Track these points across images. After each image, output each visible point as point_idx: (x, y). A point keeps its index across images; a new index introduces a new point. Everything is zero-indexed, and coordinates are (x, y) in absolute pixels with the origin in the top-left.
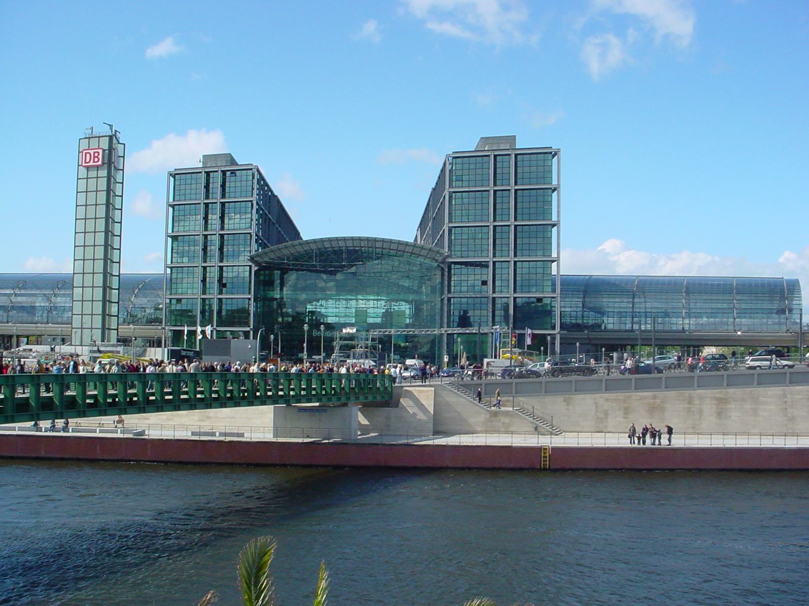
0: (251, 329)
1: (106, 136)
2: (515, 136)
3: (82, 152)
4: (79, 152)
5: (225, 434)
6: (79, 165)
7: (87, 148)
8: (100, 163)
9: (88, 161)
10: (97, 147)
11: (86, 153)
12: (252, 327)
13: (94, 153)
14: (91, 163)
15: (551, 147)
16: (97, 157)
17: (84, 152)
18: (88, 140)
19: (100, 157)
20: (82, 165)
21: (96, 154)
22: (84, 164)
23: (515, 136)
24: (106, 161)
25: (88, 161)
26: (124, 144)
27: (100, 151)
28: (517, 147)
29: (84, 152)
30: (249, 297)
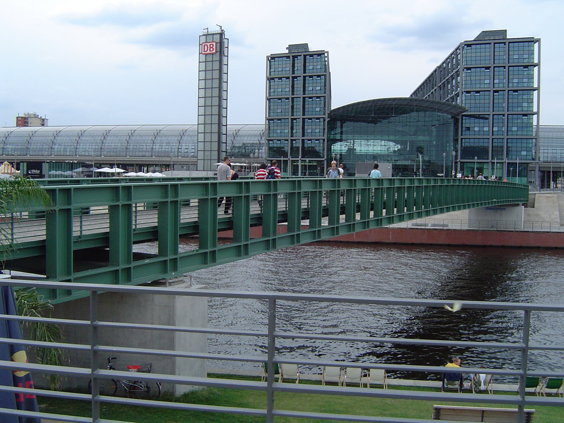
0: (325, 159)
1: (218, 34)
2: (506, 30)
3: (202, 44)
4: (200, 45)
5: (434, 225)
6: (200, 53)
7: (205, 42)
8: (214, 51)
9: (206, 50)
10: (212, 41)
11: (204, 45)
12: (326, 158)
13: (210, 45)
14: (208, 52)
15: (533, 38)
16: (212, 48)
17: (203, 44)
18: (205, 36)
19: (214, 47)
20: (202, 53)
21: (212, 46)
22: (203, 53)
23: (506, 30)
24: (218, 50)
25: (206, 50)
26: (228, 39)
27: (214, 44)
28: (507, 38)
29: (203, 44)
30: (324, 138)
